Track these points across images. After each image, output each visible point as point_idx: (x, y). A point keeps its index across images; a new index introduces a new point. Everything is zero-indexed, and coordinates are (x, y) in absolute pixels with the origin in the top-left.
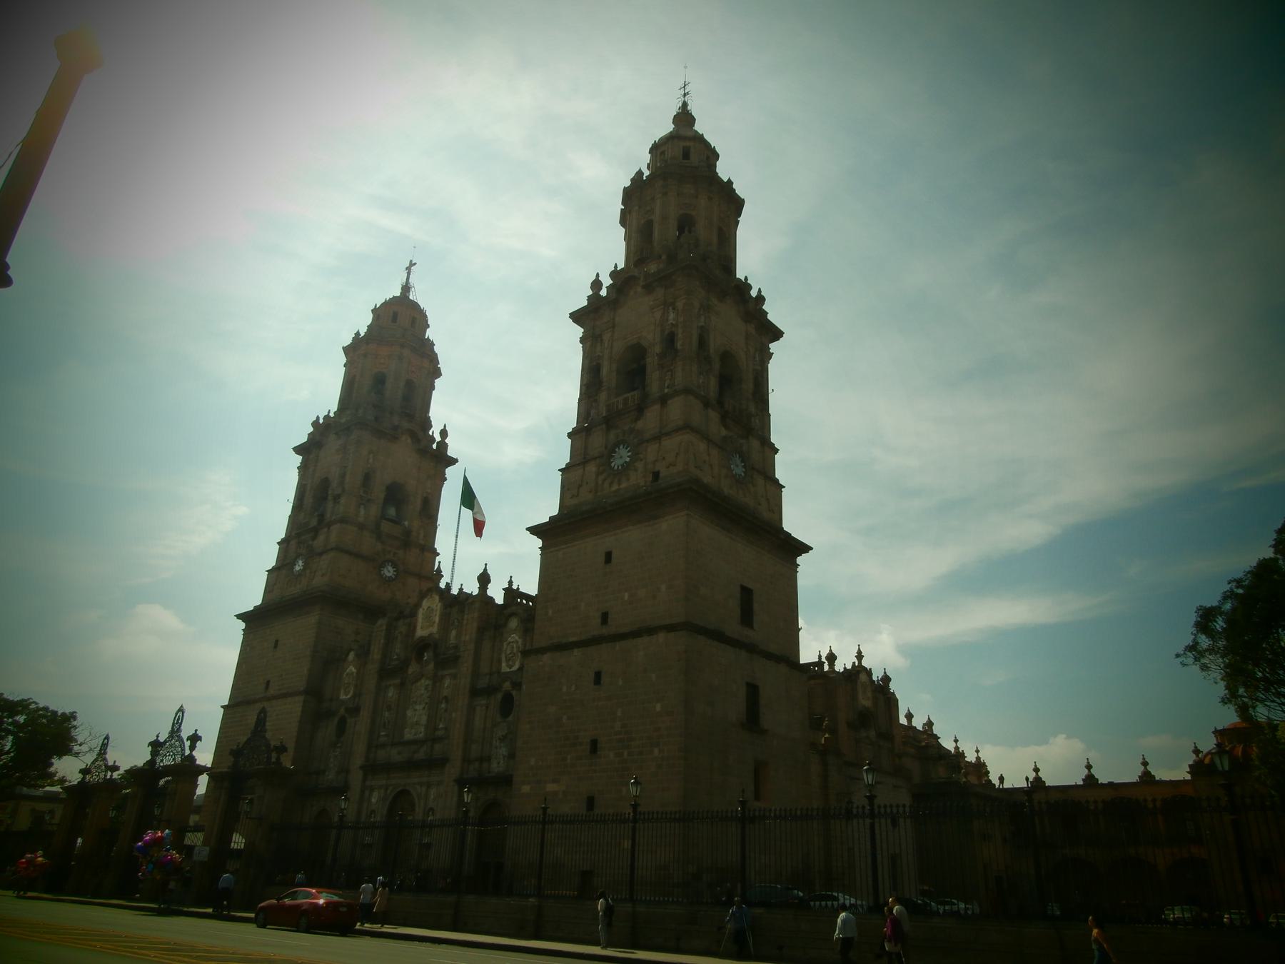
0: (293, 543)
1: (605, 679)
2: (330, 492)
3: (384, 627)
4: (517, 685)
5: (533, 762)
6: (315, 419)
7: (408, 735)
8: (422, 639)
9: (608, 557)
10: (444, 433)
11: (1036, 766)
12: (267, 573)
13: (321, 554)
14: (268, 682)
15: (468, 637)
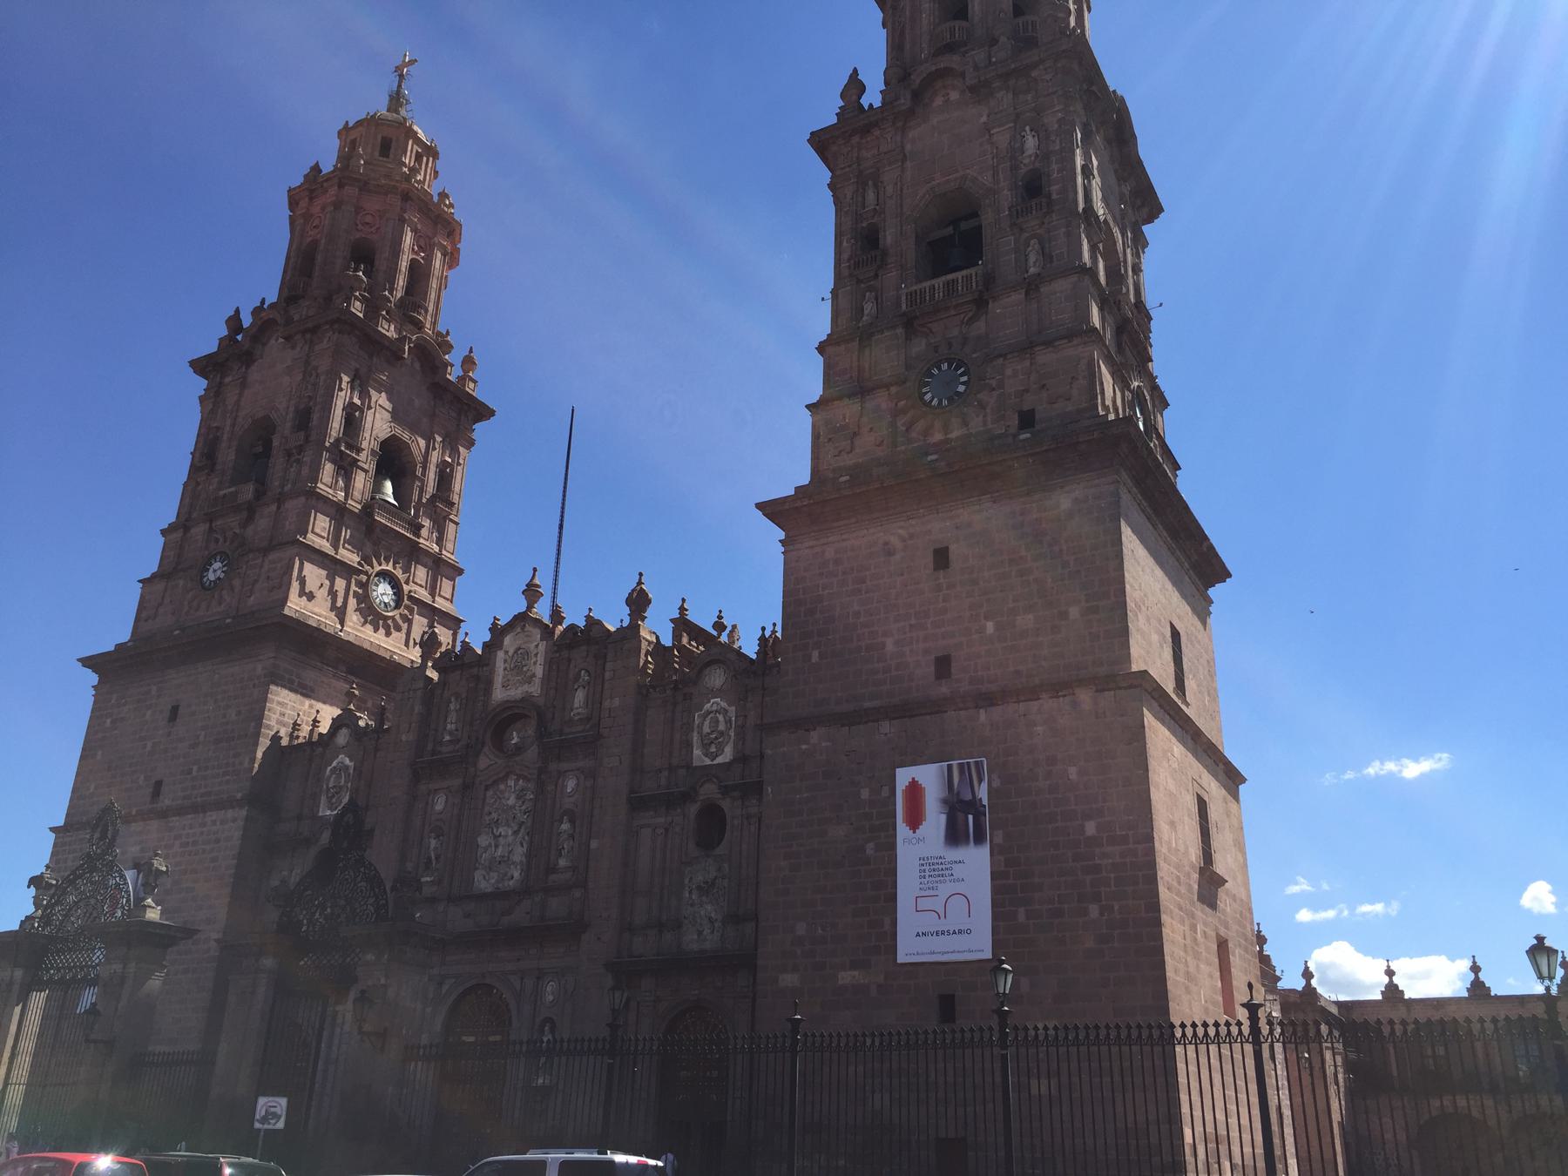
0: (199, 531)
2: (276, 443)
7: (483, 882)
8: (507, 705)
9: (941, 558)
10: (468, 362)
11: (1474, 962)
13: (265, 551)
14: (159, 784)
15: (617, 702)
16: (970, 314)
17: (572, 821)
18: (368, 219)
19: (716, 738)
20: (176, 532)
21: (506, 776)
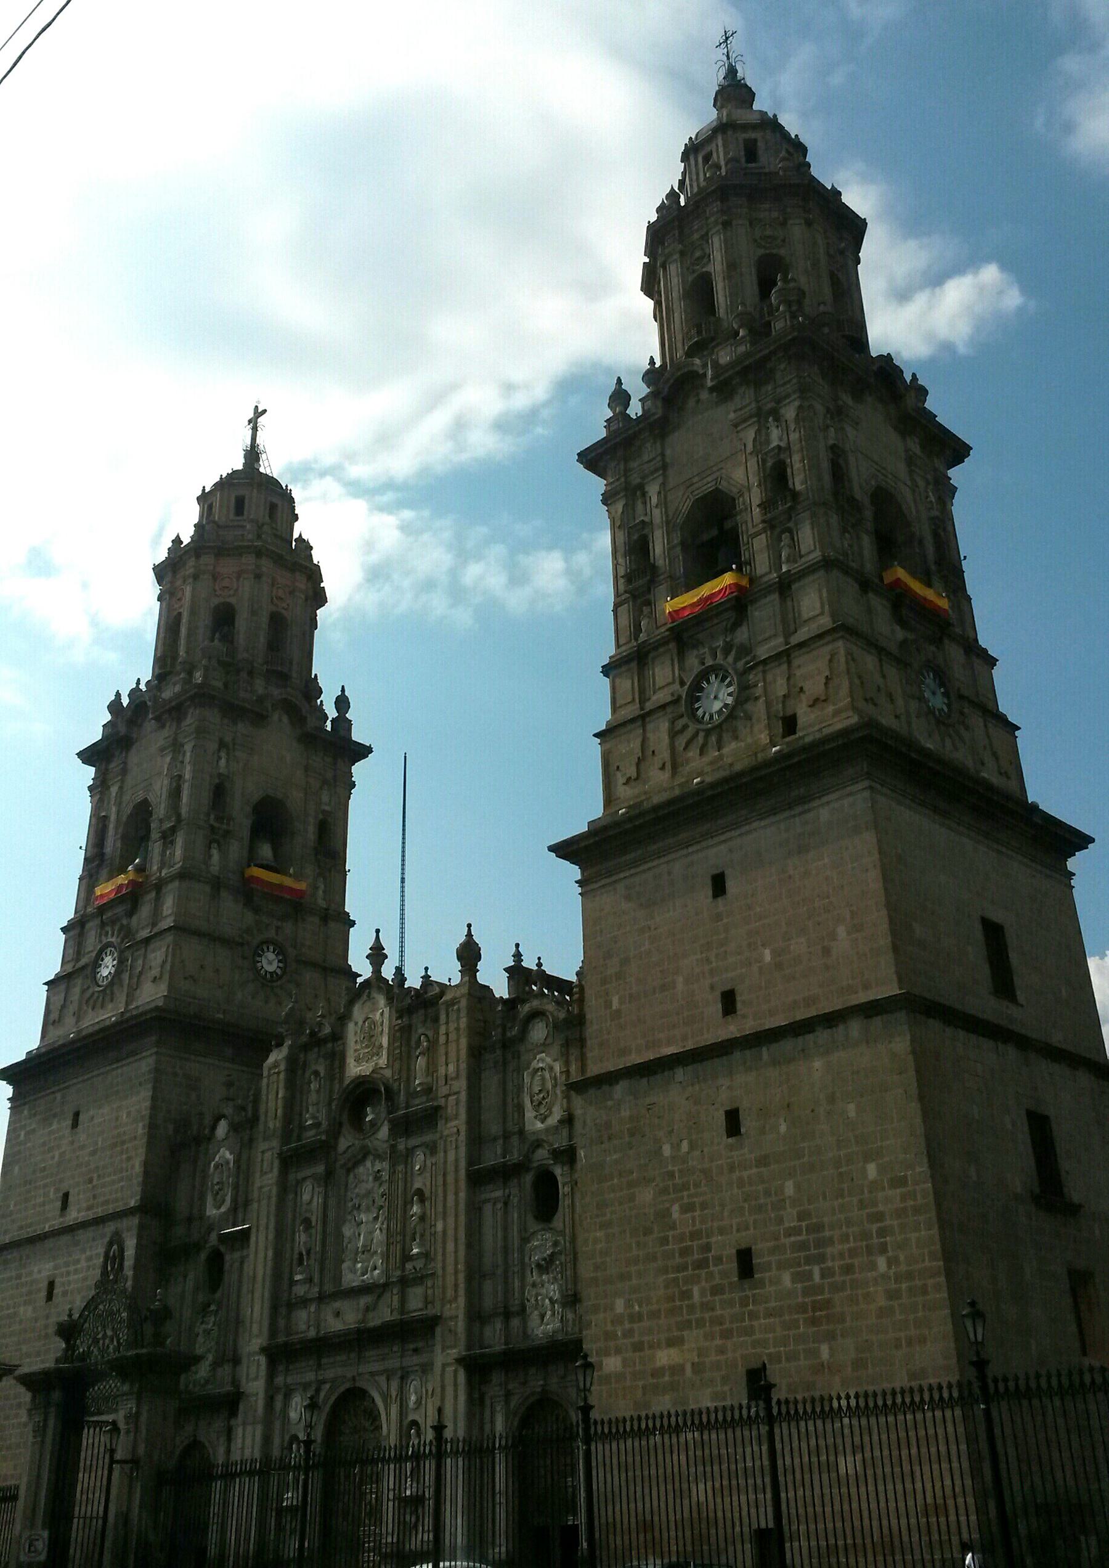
1: (748, 1124)
3: (282, 1067)
4: (568, 1155)
5: (620, 1305)
6: (113, 698)
8: (361, 1082)
12: (46, 987)
15: (451, 1068)
16: (732, 620)
17: (422, 1200)
18: (226, 583)
19: (544, 1098)
20: (74, 930)
21: (364, 1157)
